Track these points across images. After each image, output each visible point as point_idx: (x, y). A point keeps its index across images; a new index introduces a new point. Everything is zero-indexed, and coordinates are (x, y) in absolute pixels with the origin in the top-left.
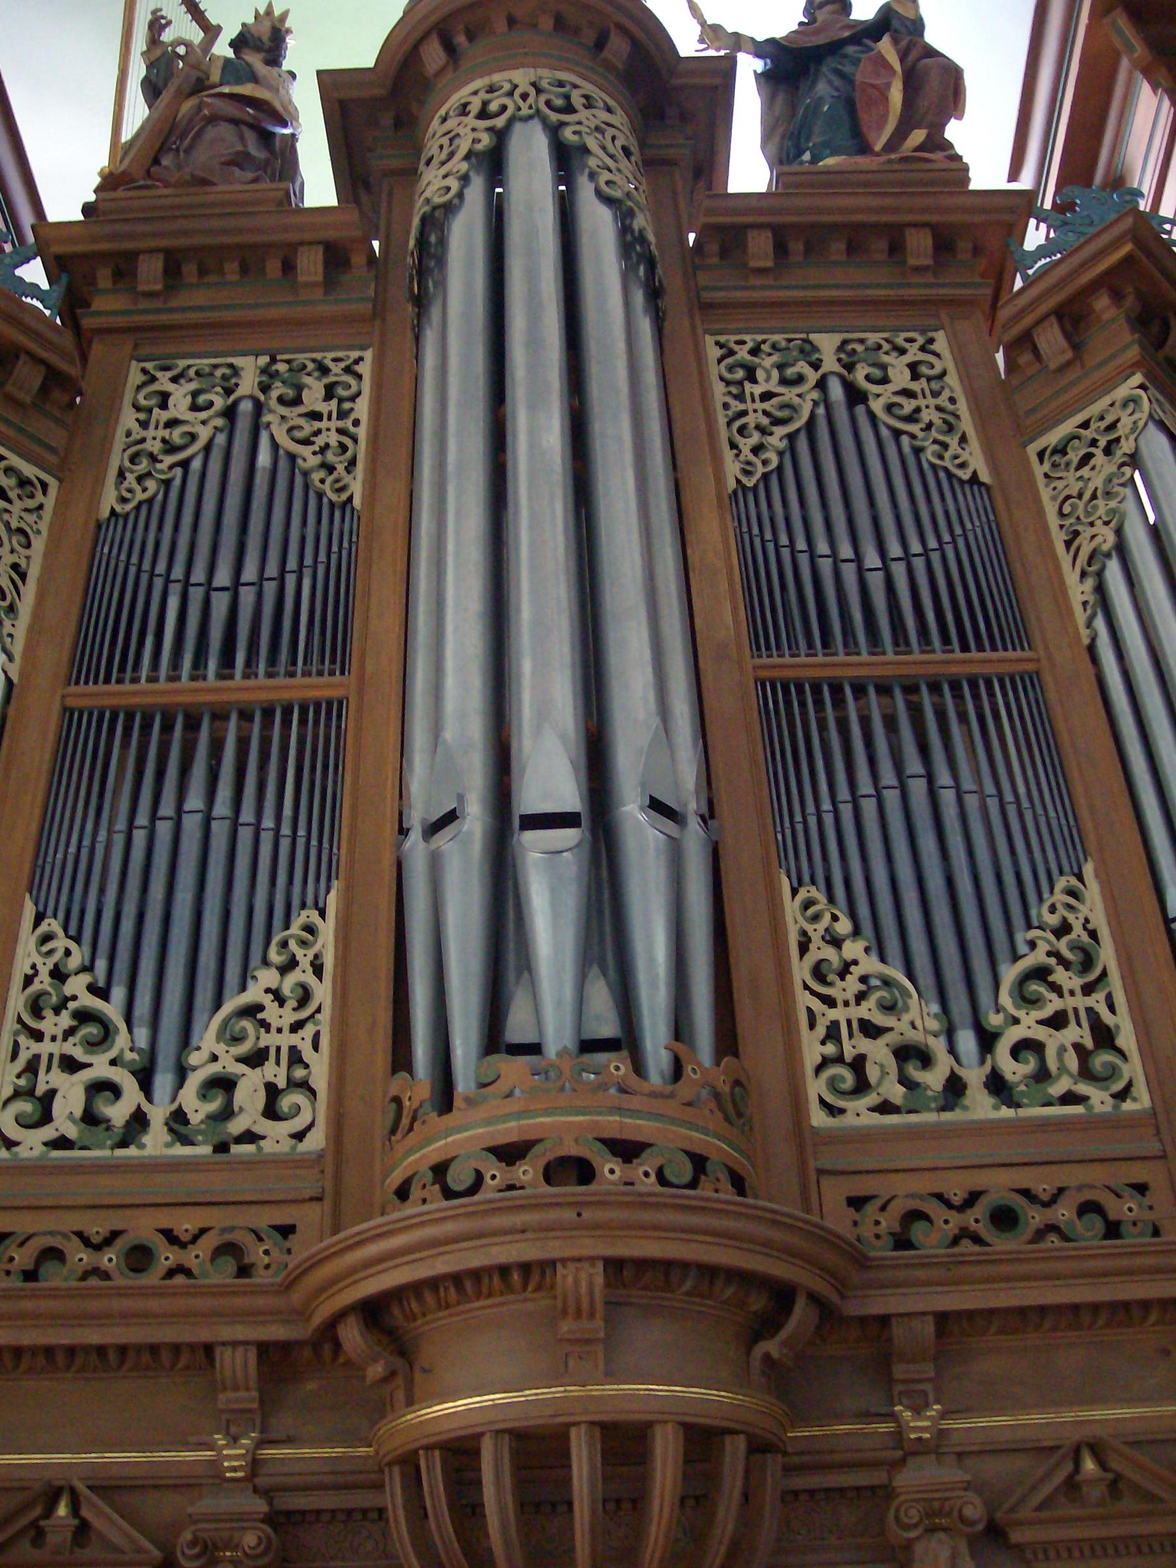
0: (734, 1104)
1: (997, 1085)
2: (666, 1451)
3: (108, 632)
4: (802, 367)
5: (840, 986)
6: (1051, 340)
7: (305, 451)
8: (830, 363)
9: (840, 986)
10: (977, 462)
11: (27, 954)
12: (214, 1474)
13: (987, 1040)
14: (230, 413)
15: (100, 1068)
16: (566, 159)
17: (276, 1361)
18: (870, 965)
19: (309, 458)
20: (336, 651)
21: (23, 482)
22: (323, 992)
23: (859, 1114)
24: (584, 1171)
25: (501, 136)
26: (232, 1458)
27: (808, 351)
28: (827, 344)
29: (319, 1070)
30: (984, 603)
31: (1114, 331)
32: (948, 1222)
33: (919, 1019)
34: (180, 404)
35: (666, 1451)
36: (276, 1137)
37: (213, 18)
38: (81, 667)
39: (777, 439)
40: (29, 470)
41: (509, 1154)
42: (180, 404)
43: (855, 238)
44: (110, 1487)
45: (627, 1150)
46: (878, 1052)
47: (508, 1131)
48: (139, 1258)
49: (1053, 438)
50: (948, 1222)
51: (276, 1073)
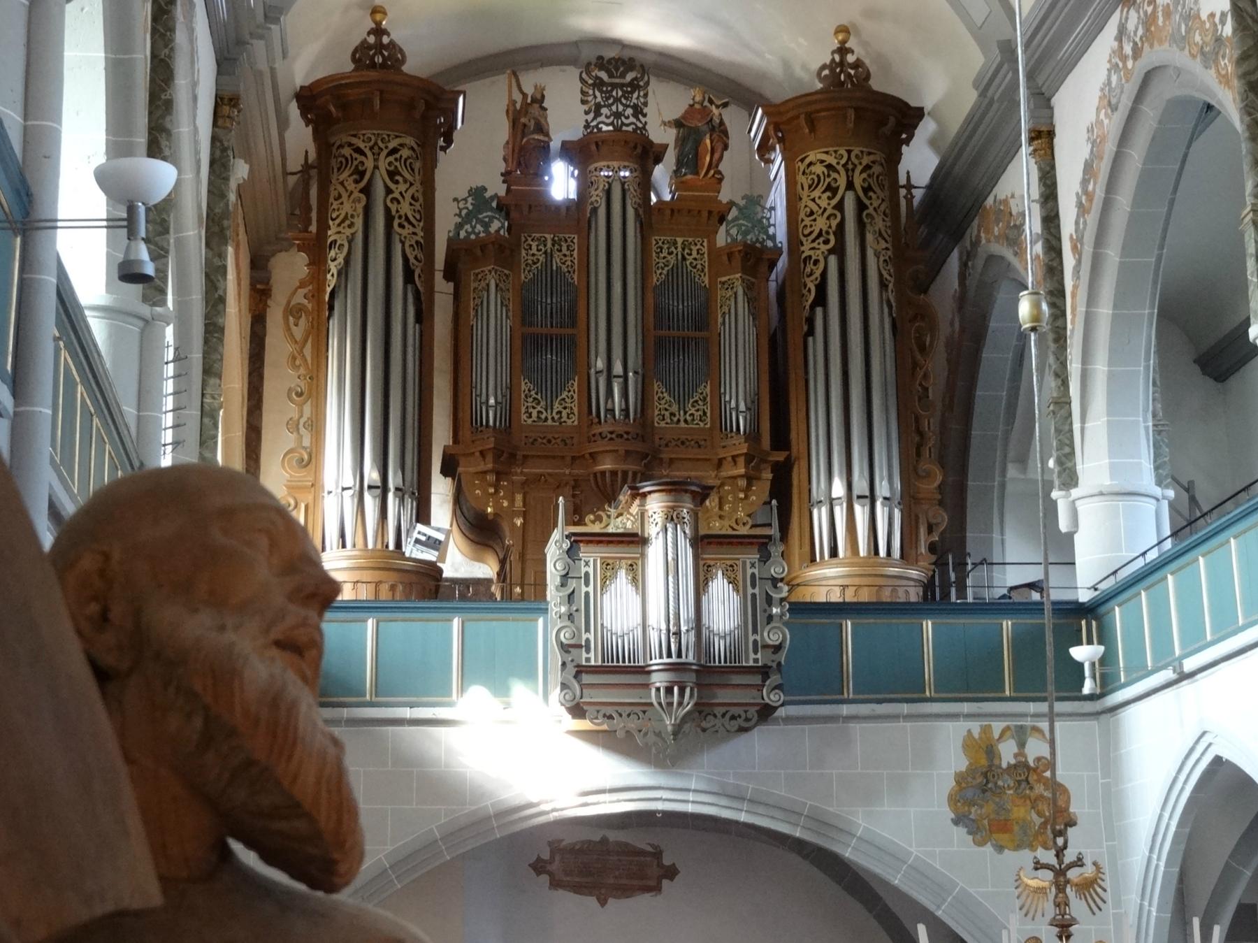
0: (644, 425)
1: (686, 421)
2: (630, 474)
3: (526, 312)
4: (673, 249)
5: (662, 401)
6: (725, 258)
7: (564, 267)
8: (680, 249)
9: (662, 401)
10: (707, 282)
11: (523, 387)
12: (564, 474)
13: (685, 413)
14: (545, 253)
15: (539, 408)
16: (624, 191)
17: (574, 458)
18: (667, 398)
19: (564, 268)
20: (574, 324)
21: (507, 276)
22: (576, 396)
23: (663, 424)
24: (621, 436)
25: (610, 184)
26: (567, 472)
27: (675, 243)
28: (680, 240)
29: (576, 410)
30: (702, 319)
31: (737, 260)
32: (674, 443)
33: (675, 408)
34: (534, 250)
35: (630, 474)
36: (569, 422)
37: (525, 90)
38: (523, 323)
39: (665, 272)
40: (506, 272)
41: (611, 433)
42: (534, 250)
43: (689, 211)
44: (550, 474)
45: (627, 433)
46: (667, 414)
47: (611, 429)
48: (549, 441)
49: (724, 279)
50: (674, 443)
51: (568, 410)
